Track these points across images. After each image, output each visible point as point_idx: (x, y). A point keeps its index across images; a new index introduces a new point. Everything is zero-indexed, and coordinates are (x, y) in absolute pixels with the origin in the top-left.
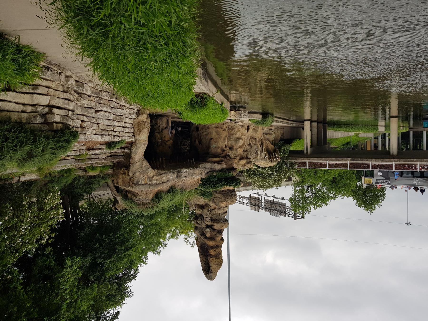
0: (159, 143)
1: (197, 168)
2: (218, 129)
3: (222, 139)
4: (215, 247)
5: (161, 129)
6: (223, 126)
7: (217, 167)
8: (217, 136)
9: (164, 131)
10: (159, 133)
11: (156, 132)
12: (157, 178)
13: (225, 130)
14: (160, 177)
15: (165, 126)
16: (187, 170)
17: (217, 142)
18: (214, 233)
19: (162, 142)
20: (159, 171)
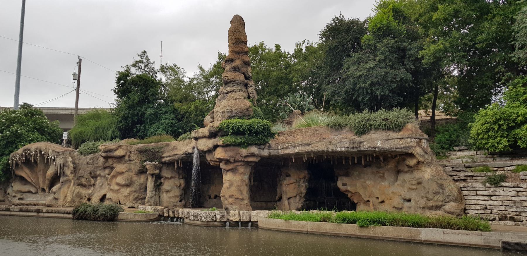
0: (302, 180)
1: (323, 151)
2: (241, 197)
3: (235, 184)
4: (242, 53)
5: (298, 197)
6: (234, 201)
7: (254, 149)
8: (242, 189)
9: (295, 195)
10: (302, 193)
11: (304, 194)
12: (411, 144)
13: (231, 196)
14: (407, 145)
15: (292, 201)
16: (338, 149)
17: (243, 181)
18: (244, 69)
19: (299, 183)
20: (406, 151)
